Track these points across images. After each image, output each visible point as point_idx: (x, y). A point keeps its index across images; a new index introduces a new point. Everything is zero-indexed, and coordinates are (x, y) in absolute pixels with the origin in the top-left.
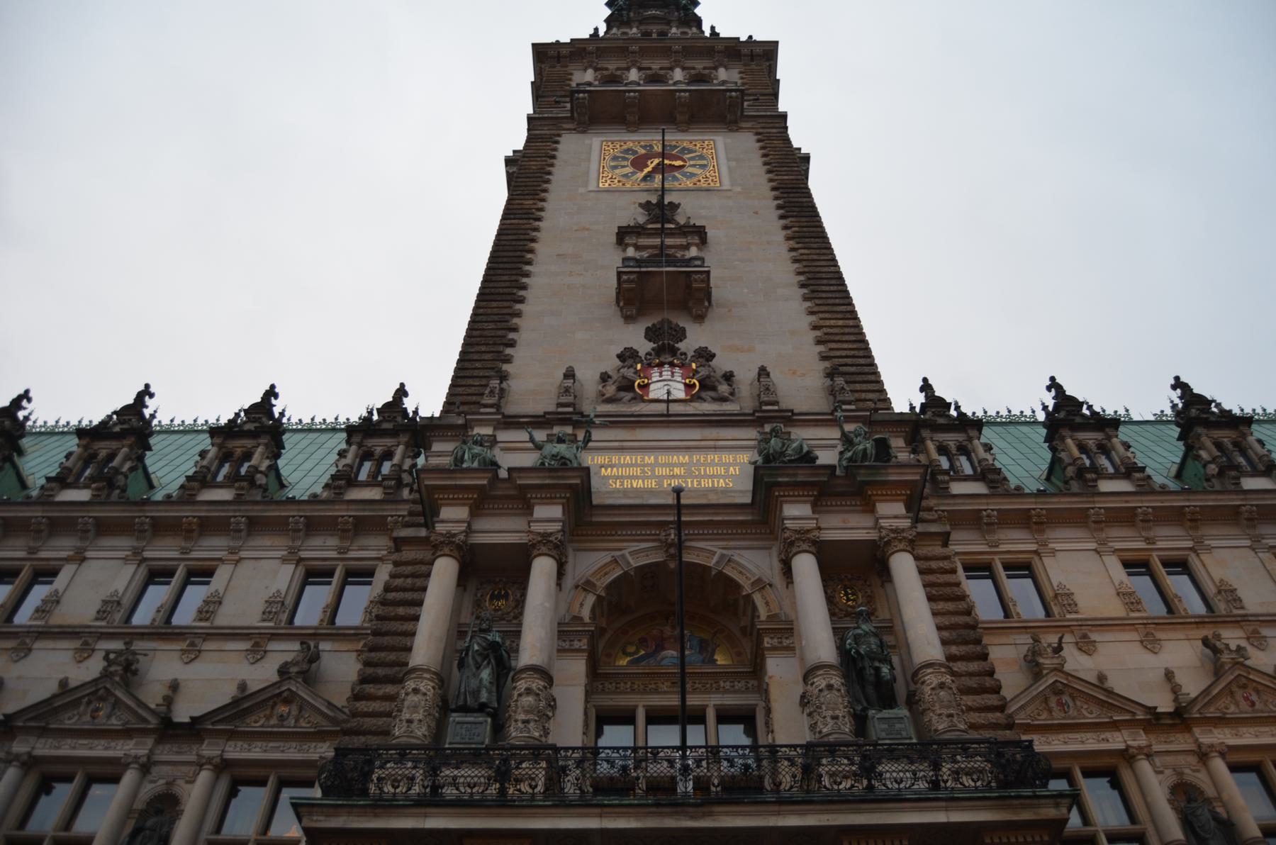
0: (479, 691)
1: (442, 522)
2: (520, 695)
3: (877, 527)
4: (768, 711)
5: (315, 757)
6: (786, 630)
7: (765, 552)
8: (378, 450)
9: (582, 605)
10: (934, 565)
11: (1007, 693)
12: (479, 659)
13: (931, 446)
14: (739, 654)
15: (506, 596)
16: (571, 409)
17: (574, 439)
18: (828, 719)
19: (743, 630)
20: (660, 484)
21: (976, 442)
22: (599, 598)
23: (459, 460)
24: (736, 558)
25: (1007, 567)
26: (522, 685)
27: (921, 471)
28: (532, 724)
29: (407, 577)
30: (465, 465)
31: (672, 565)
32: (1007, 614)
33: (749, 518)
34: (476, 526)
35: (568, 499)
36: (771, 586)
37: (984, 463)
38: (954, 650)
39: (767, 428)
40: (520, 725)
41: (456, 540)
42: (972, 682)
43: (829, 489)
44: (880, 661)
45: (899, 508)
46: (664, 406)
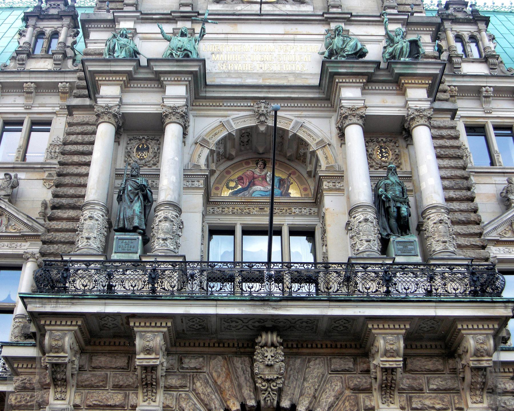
0: (133, 218)
1: (102, 97)
2: (160, 221)
3: (406, 106)
4: (324, 232)
5: (21, 252)
6: (339, 177)
7: (327, 120)
8: (48, 31)
9: (199, 156)
10: (444, 132)
11: (485, 218)
12: (132, 196)
13: (451, 36)
14: (305, 189)
15: (148, 149)
16: (189, 9)
17: (193, 32)
18: (364, 242)
19: (309, 173)
21: (484, 33)
22: (212, 152)
23: (112, 51)
24: (307, 124)
25: (496, 128)
26: (161, 214)
27: (441, 67)
28: (169, 241)
29: (78, 134)
30: (116, 55)
31: (262, 128)
32: (492, 163)
33: (316, 96)
34: (125, 101)
35: (189, 81)
36: (329, 145)
37: (487, 50)
38: (452, 194)
39: (333, 26)
40: (161, 242)
41: (112, 111)
42: (462, 217)
43: (372, 78)
44: (401, 203)
45: (422, 93)
46: (257, 7)
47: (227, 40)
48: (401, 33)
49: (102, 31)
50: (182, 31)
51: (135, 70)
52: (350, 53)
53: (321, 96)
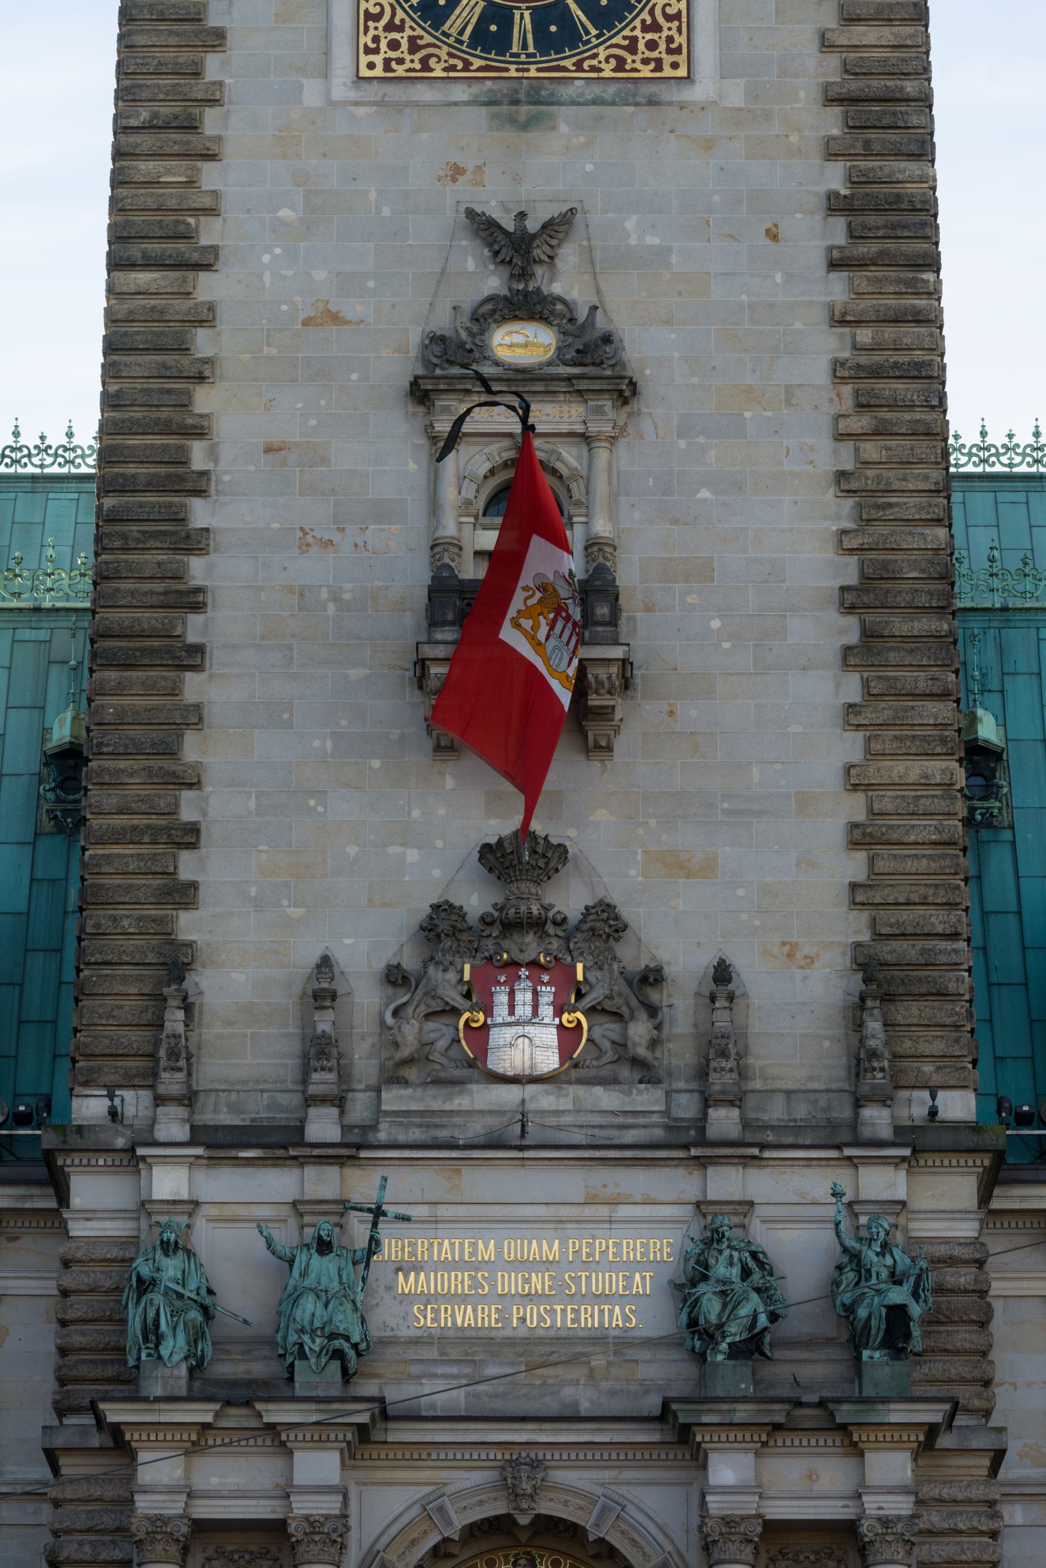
20: (504, 1317)
27: (947, 1407)
31: (524, 1520)
33: (656, 1438)
35: (349, 1443)
47: (436, 1222)
48: (882, 1234)
49: (100, 1173)
50: (320, 1238)
51: (217, 1415)
52: (738, 1339)
53: (668, 1438)
